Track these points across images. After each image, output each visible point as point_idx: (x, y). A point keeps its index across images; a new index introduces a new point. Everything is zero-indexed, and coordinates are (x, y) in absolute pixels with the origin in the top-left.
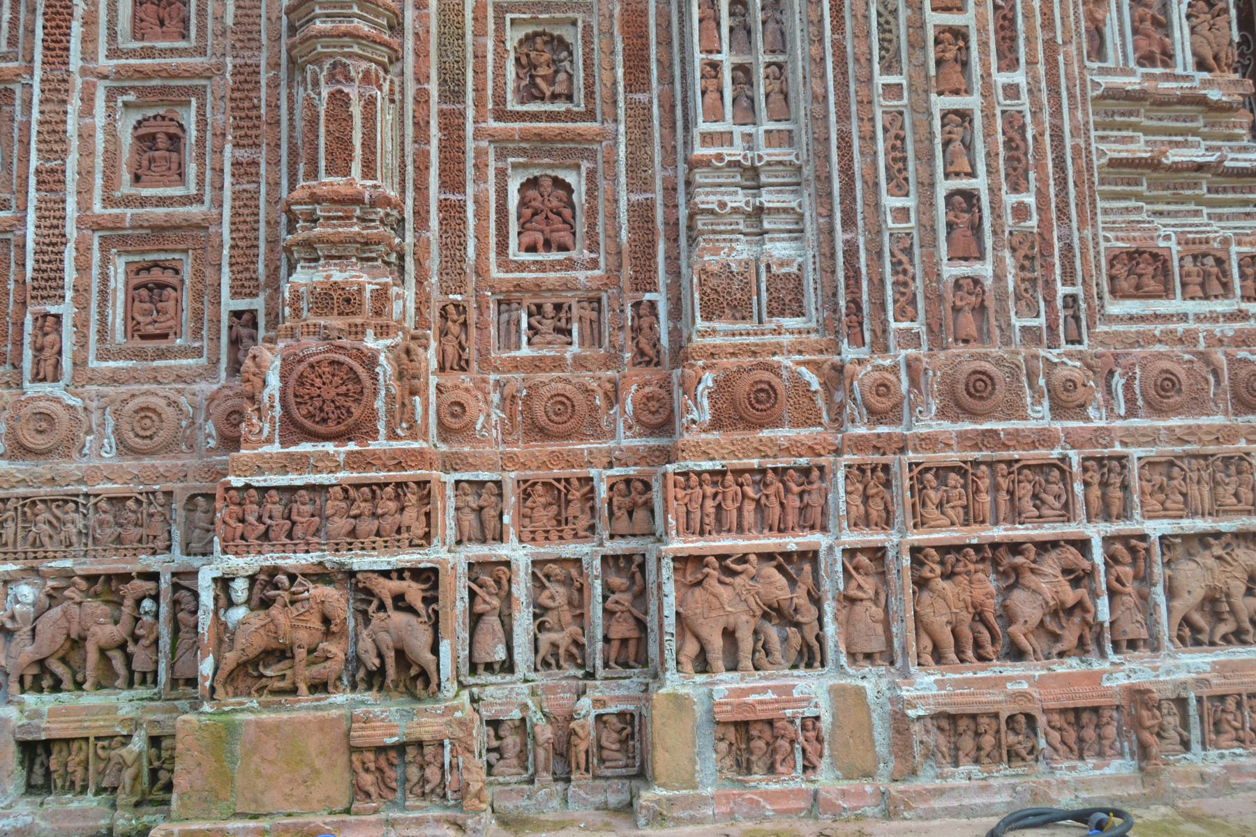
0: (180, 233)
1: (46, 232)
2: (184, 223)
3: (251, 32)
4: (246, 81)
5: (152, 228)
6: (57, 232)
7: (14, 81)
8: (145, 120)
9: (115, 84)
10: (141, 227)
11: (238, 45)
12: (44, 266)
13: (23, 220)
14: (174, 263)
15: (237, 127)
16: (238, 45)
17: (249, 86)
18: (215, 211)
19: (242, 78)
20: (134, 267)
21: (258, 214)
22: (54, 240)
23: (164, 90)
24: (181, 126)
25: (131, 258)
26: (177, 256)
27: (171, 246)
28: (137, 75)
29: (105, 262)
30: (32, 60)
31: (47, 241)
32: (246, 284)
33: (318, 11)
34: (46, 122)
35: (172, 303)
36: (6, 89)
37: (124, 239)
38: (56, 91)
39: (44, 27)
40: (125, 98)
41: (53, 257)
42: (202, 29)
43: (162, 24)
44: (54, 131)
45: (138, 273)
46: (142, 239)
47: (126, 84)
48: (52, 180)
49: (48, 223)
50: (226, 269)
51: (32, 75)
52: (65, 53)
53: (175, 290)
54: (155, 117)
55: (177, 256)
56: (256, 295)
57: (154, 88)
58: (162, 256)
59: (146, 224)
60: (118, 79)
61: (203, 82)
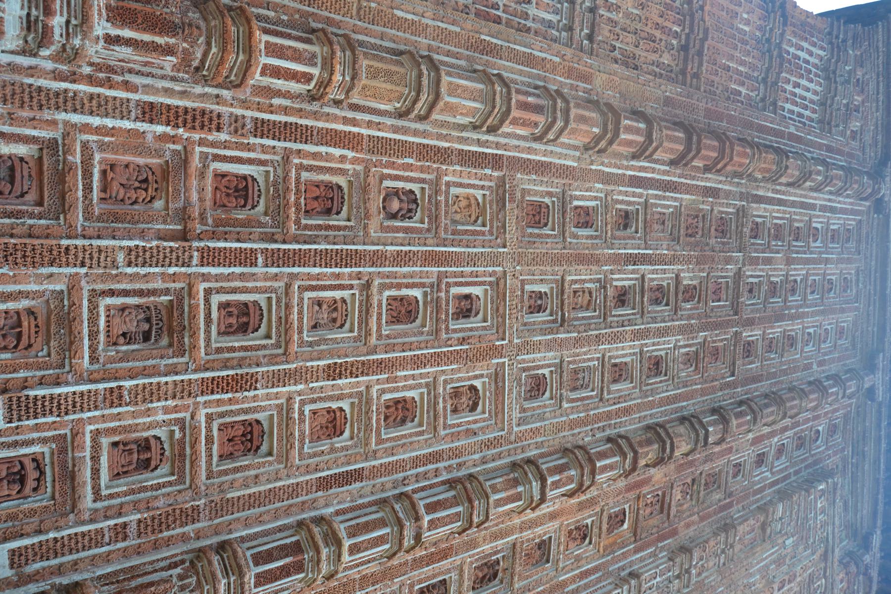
0: (69, 491)
1: (70, 399)
2: (77, 496)
3: (222, 510)
4: (187, 516)
5: (73, 472)
6: (70, 407)
7: (190, 357)
8: (161, 442)
9: (187, 424)
10: (74, 465)
11: (213, 504)
12: (39, 403)
13: (80, 380)
14: (43, 487)
15: (153, 518)
16: (213, 504)
17: (184, 519)
18: (86, 516)
19: (190, 513)
20: (39, 458)
21: (83, 550)
22: (63, 407)
23: (182, 455)
24: (156, 468)
25: (47, 456)
26: (49, 490)
27: (57, 487)
28: (193, 439)
29: (44, 441)
30: (207, 369)
31: (62, 402)
32: (23, 558)
33: (232, 579)
34: (159, 387)
35: (7, 493)
36: (185, 350)
37: (63, 451)
38: (184, 390)
39: (228, 376)
40: (177, 432)
41: (48, 409)
42: (225, 473)
43: (229, 440)
44: (152, 393)
45: (34, 460)
46: (63, 465)
47: (187, 431)
48: (115, 398)
49: (77, 399)
50: (36, 540)
51: (195, 371)
52: (209, 392)
53: (18, 492)
54: (163, 448)
55: (49, 490)
56: (12, 567)
57: (184, 448)
58: (49, 479)
59: (76, 469)
60: (190, 425)
61: (188, 482)
